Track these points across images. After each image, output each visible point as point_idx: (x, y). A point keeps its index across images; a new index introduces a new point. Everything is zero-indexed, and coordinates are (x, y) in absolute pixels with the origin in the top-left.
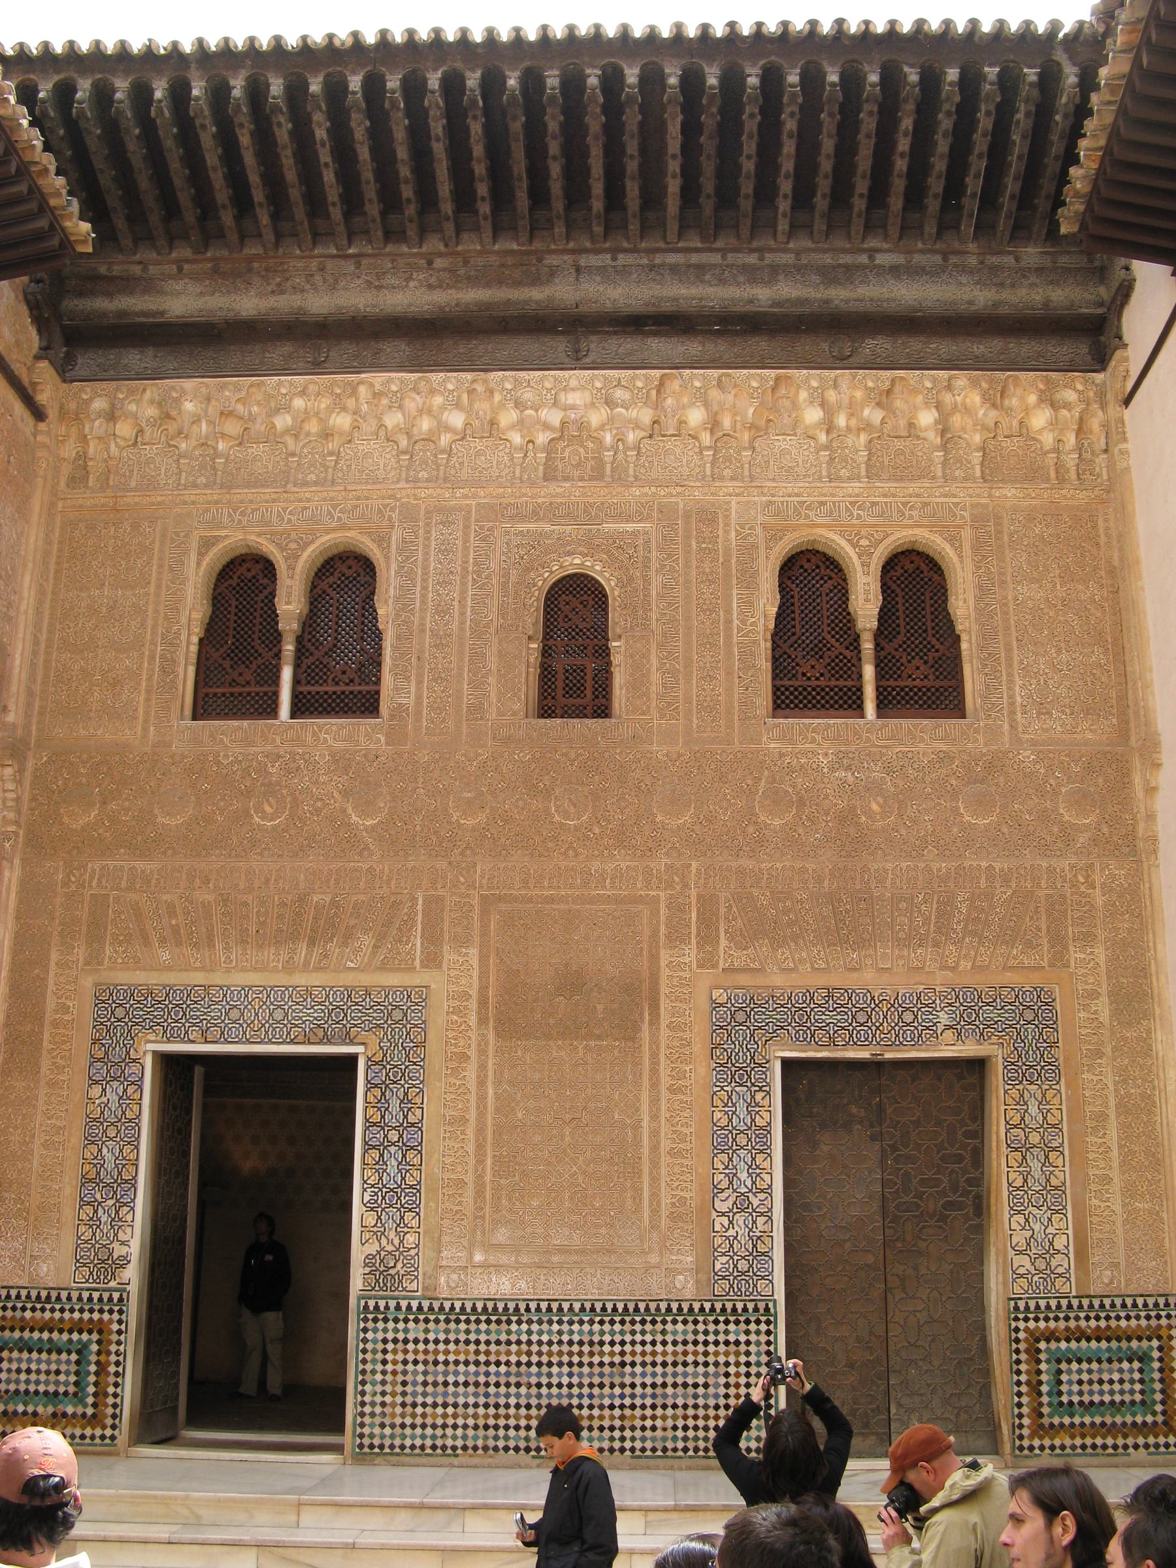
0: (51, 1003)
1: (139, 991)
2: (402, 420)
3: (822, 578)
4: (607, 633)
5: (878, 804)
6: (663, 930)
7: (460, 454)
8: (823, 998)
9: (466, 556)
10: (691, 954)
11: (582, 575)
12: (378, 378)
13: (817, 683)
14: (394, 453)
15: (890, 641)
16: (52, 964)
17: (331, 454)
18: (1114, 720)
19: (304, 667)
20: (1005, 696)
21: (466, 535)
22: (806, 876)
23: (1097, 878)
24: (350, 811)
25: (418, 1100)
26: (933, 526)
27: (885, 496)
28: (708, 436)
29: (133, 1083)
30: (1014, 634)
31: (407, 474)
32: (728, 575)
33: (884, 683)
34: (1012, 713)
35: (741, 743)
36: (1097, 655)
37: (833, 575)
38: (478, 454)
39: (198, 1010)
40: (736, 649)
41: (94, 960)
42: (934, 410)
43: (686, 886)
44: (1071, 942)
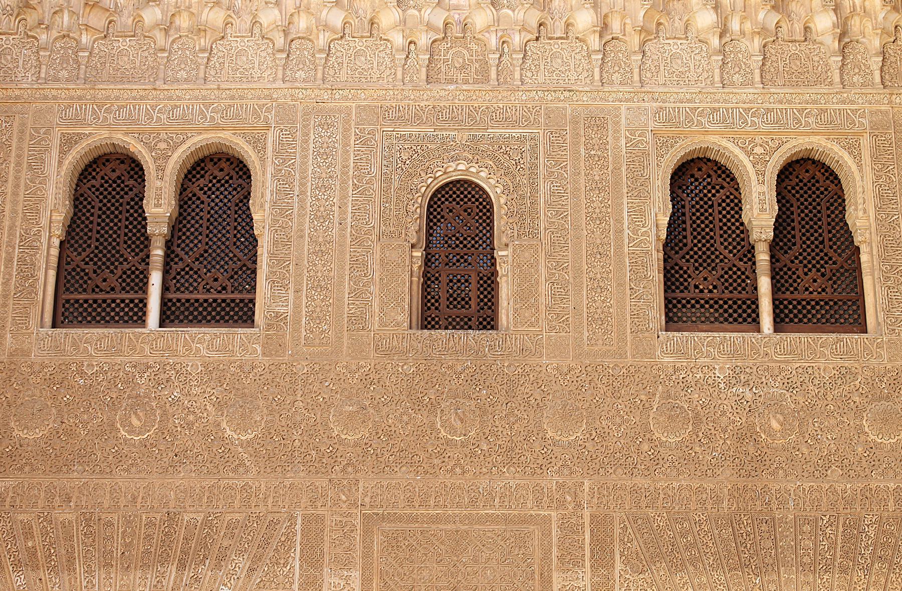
2: (279, 17)
3: (713, 188)
4: (492, 242)
5: (778, 421)
6: (555, 550)
7: (339, 54)
11: (466, 181)
14: (270, 51)
15: (786, 252)
17: (203, 50)
19: (173, 273)
21: (346, 137)
22: (704, 496)
24: (224, 425)
26: (830, 134)
27: (781, 102)
28: (597, 39)
31: (284, 74)
32: (617, 183)
33: (780, 296)
35: (633, 356)
37: (725, 184)
38: (357, 54)
42: (832, 14)
43: (579, 505)
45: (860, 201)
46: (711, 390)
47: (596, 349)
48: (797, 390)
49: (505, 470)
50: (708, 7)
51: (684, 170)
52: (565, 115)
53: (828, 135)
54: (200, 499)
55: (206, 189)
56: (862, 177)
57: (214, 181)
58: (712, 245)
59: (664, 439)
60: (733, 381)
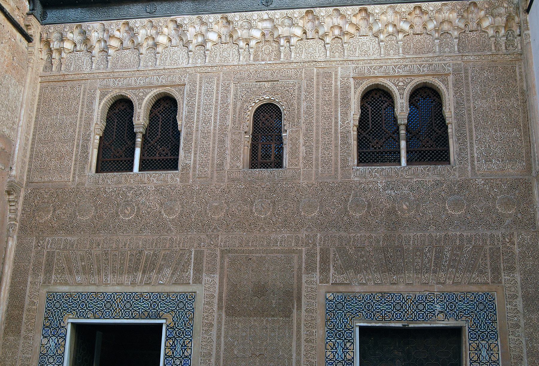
0: (27, 300)
1: (66, 295)
3: (382, 102)
4: (281, 130)
5: (406, 205)
7: (216, 51)
8: (379, 298)
9: (217, 97)
10: (317, 276)
11: (271, 104)
12: (179, 19)
14: (186, 51)
16: (29, 283)
18: (524, 164)
22: (372, 240)
23: (516, 240)
24: (163, 212)
25: (189, 345)
27: (411, 62)
29: (62, 337)
30: (473, 124)
32: (336, 102)
36: (515, 132)
39: (92, 304)
40: (339, 135)
41: (47, 282)
44: (502, 271)
45: (448, 105)
53: (433, 75)
54: (152, 244)
55: (160, 112)
56: (449, 94)
57: (164, 109)
58: (381, 128)
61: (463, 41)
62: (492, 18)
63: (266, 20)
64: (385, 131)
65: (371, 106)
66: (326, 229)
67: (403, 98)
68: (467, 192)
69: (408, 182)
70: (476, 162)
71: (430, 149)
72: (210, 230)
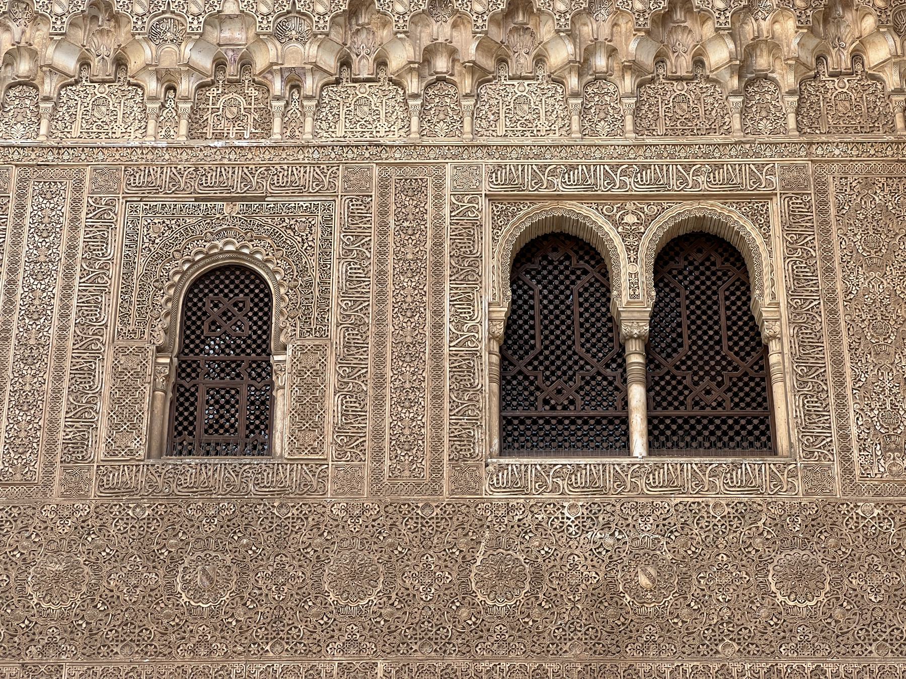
3: (573, 273)
4: (268, 346)
5: (649, 576)
9: (73, 239)
13: (566, 413)
15: (669, 355)
20: (834, 426)
21: (75, 209)
27: (660, 156)
28: (415, 80)
30: (845, 341)
32: (438, 265)
34: (846, 450)
35: (452, 492)
37: (588, 268)
45: (767, 284)
46: (558, 536)
47: (401, 482)
48: (676, 534)
49: (268, 648)
50: (562, 34)
51: (534, 250)
52: (371, 178)
58: (569, 347)
59: (490, 603)
60: (589, 523)
61: (812, 103)
62: (897, 38)
63: (230, 17)
64: (581, 358)
65: (539, 282)
66: (403, 648)
67: (636, 261)
68: (832, 541)
69: (654, 508)
70: (856, 453)
71: (715, 413)
72: (33, 649)
